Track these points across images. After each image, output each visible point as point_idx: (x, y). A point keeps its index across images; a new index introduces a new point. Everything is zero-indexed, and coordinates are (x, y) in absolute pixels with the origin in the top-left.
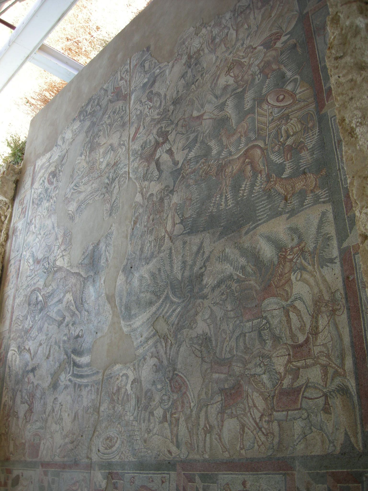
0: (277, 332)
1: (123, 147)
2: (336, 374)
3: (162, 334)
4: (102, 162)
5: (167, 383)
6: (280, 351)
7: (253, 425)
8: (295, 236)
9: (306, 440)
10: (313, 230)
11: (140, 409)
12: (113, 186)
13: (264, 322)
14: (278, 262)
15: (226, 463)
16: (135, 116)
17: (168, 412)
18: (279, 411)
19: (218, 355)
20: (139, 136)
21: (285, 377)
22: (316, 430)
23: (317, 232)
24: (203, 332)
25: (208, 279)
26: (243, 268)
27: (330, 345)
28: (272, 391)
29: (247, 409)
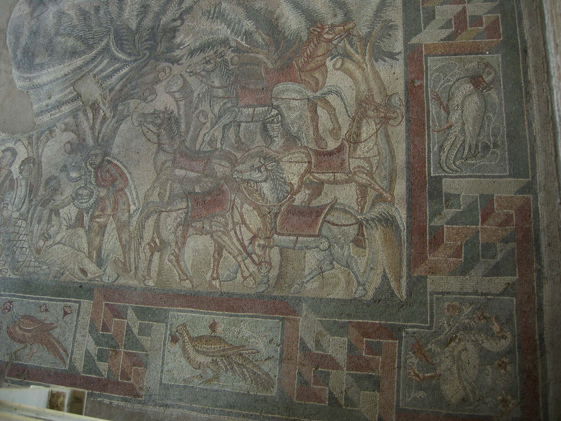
0: (294, 129)
2: (379, 198)
3: (89, 101)
5: (90, 171)
6: (296, 155)
7: (237, 248)
8: (338, 11)
9: (323, 278)
10: (369, 11)
11: (34, 202)
13: (274, 112)
14: (308, 39)
15: (185, 296)
17: (88, 213)
18: (283, 235)
19: (188, 144)
21: (298, 191)
22: (339, 266)
23: (374, 14)
24: (166, 108)
25: (185, 37)
26: (248, 35)
27: (375, 161)
28: (275, 206)
29: (230, 226)
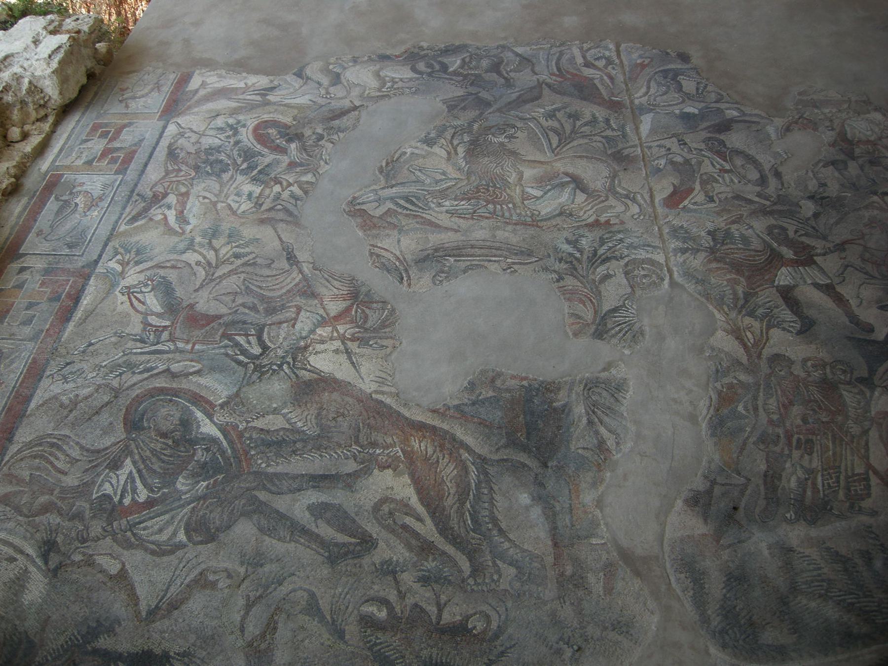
1: (629, 203)
4: (537, 198)
12: (601, 270)
16: (663, 162)
20: (691, 206)
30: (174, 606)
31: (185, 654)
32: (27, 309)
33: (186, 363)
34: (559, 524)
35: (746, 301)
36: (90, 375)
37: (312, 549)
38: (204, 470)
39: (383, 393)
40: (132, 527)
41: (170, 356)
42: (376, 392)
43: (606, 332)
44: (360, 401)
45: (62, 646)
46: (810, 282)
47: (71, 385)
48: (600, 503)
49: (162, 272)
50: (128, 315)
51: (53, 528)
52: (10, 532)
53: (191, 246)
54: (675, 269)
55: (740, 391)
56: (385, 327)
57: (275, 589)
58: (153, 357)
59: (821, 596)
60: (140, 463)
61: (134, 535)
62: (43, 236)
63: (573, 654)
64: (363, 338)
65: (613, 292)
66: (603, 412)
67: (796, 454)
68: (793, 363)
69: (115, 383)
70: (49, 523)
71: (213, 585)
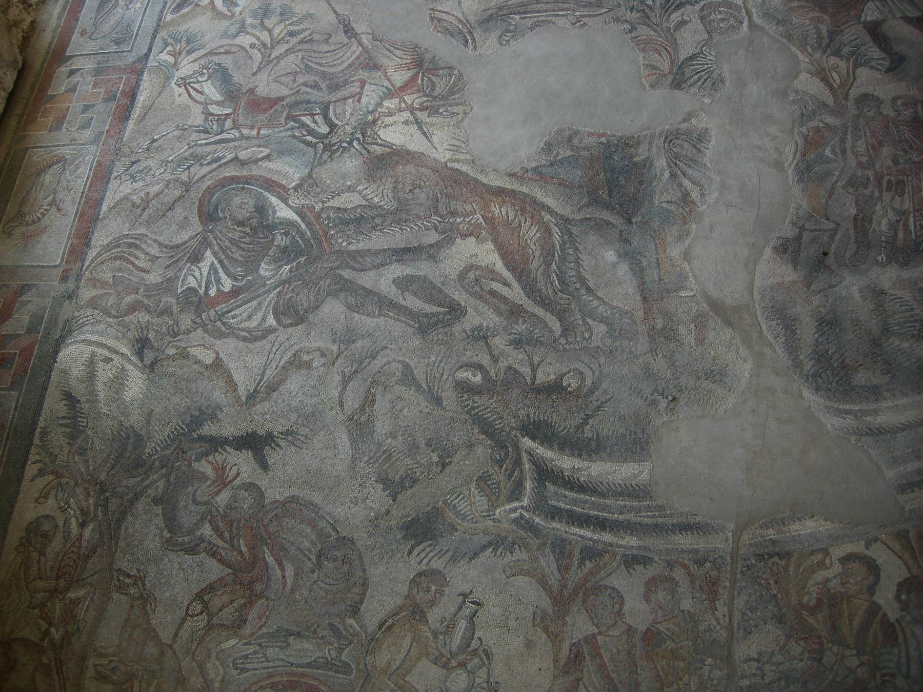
12: (675, 17)
30: (272, 388)
31: (288, 433)
32: (83, 112)
33: (254, 149)
34: (647, 279)
35: (831, 40)
36: (158, 172)
37: (402, 322)
38: (286, 254)
39: (458, 161)
40: (221, 316)
41: (236, 143)
42: (451, 160)
43: (685, 82)
44: (435, 171)
45: (168, 436)
46: (898, 15)
47: (141, 184)
48: (687, 256)
49: (216, 59)
50: (187, 107)
51: (143, 326)
52: (102, 334)
53: (242, 29)
54: (754, 10)
55: (826, 134)
56: (453, 93)
57: (369, 363)
58: (219, 147)
59: (913, 336)
60: (220, 254)
61: (224, 324)
62: (88, 35)
63: (669, 405)
64: (432, 107)
65: (689, 40)
66: (686, 164)
67: (887, 196)
68: (882, 102)
69: (184, 177)
70: (139, 322)
71: (308, 365)
